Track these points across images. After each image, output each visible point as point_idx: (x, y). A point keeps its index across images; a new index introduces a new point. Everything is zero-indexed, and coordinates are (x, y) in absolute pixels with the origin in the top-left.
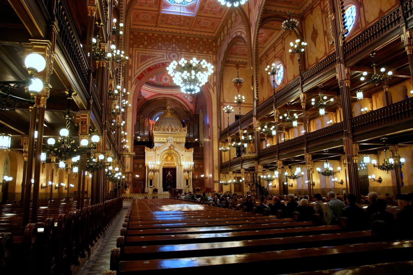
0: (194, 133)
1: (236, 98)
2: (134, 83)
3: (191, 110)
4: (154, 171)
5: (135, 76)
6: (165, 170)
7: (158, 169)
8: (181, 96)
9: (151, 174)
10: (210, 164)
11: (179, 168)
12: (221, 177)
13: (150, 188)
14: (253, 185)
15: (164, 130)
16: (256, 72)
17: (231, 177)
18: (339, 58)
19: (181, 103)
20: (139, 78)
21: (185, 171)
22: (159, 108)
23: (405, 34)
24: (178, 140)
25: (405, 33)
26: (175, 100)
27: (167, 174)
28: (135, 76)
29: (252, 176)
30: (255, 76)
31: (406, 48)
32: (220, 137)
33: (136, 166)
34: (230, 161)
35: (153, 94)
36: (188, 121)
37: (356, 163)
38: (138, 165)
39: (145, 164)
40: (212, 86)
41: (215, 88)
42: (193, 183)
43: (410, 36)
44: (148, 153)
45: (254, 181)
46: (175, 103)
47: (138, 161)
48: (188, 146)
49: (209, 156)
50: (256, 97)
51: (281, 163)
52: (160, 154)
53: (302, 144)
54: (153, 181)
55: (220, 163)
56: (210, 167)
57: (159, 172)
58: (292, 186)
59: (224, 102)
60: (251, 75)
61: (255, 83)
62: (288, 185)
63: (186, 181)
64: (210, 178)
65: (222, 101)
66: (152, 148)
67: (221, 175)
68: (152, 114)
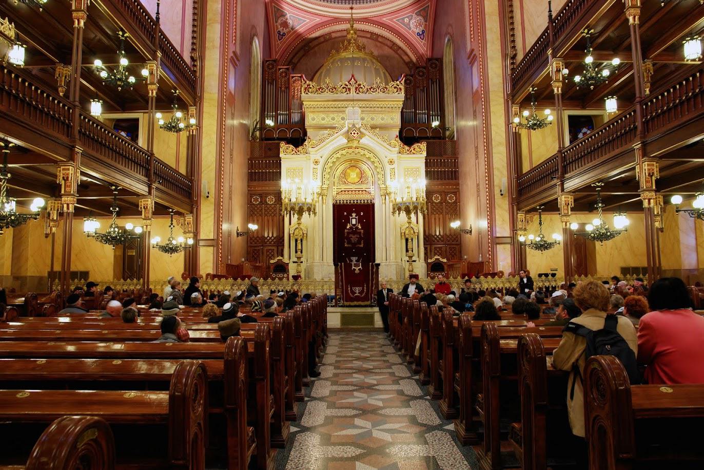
0: (428, 109)
3: (420, 57)
6: (341, 211)
7: (309, 200)
8: (391, 20)
10: (478, 185)
12: (520, 224)
13: (294, 262)
15: (333, 89)
19: (394, 44)
21: (398, 208)
24: (378, 120)
26: (378, 35)
27: (348, 221)
32: (514, 86)
34: (560, 151)
35: (318, 20)
38: (263, 196)
39: (278, 195)
42: (426, 249)
44: (289, 158)
46: (379, 44)
47: (267, 187)
48: (407, 139)
49: (477, 158)
52: (322, 161)
55: (514, 175)
56: (478, 196)
63: (404, 241)
64: (480, 233)
66: (302, 144)
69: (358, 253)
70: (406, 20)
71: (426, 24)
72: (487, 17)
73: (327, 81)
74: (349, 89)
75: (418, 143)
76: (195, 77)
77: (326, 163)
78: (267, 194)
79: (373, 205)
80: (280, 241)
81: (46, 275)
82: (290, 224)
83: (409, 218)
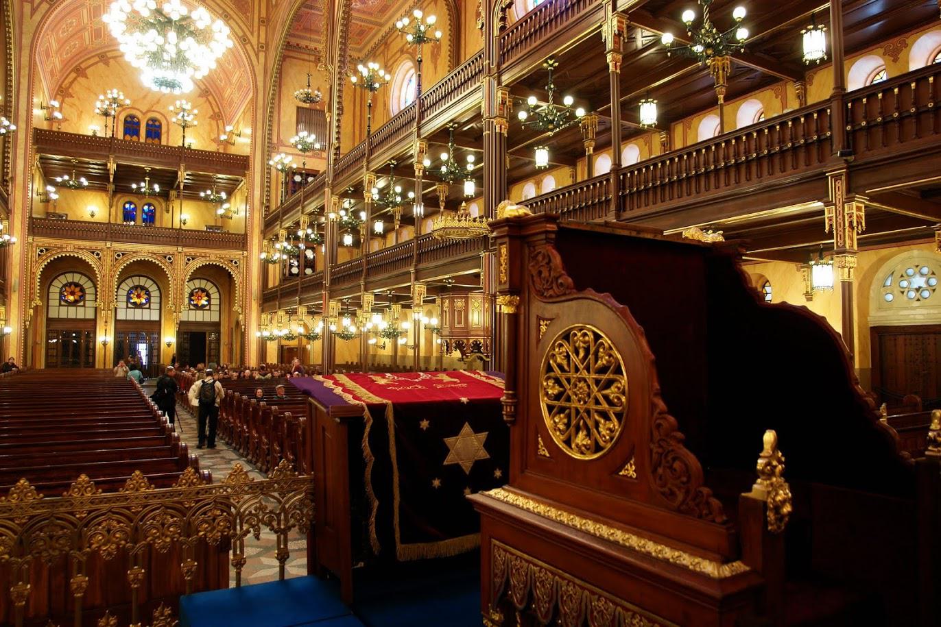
16: (340, 79)
17: (281, 323)
18: (489, 64)
23: (610, 24)
25: (609, 21)
30: (336, 88)
31: (609, 57)
37: (500, 313)
43: (619, 31)
50: (335, 141)
51: (423, 289)
53: (405, 260)
59: (281, 143)
60: (328, 87)
61: (335, 105)
65: (275, 140)
67: (264, 316)
76: (8, 195)
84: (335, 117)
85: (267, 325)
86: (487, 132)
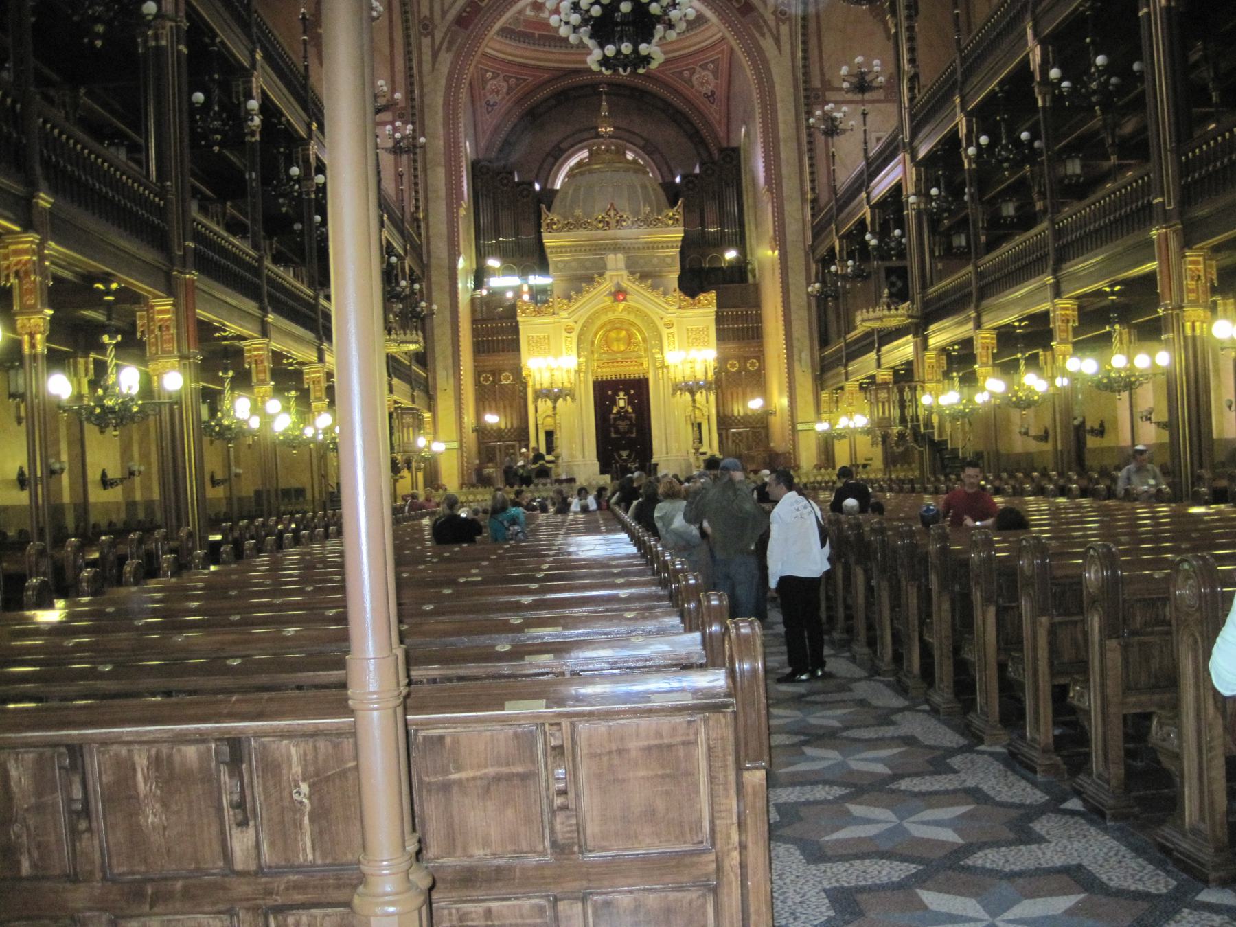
1: (844, 70)
2: (445, 45)
4: (554, 395)
5: (444, 13)
6: (604, 391)
7: (567, 385)
9: (545, 406)
11: (656, 375)
12: (824, 407)
14: (902, 436)
20: (462, 21)
21: (678, 388)
22: (580, 131)
27: (614, 403)
28: (444, 13)
29: (895, 396)
33: (486, 379)
36: (696, 176)
37: (1194, 338)
38: (495, 373)
39: (517, 371)
40: (772, 23)
41: (784, 29)
42: (720, 435)
45: (903, 420)
50: (906, 66)
52: (578, 327)
54: (558, 435)
57: (573, 399)
58: (1100, 432)
59: (827, 86)
62: (1088, 427)
67: (825, 395)
68: (550, 159)
69: (630, 445)
70: (686, 74)
71: (716, 86)
72: (782, 144)
73: (578, 212)
74: (608, 223)
75: (704, 291)
77: (582, 329)
78: (501, 372)
79: (647, 380)
80: (522, 434)
81: (252, 494)
82: (536, 411)
83: (694, 401)
84: (904, 24)
85: (831, 412)
86: (1145, 10)
